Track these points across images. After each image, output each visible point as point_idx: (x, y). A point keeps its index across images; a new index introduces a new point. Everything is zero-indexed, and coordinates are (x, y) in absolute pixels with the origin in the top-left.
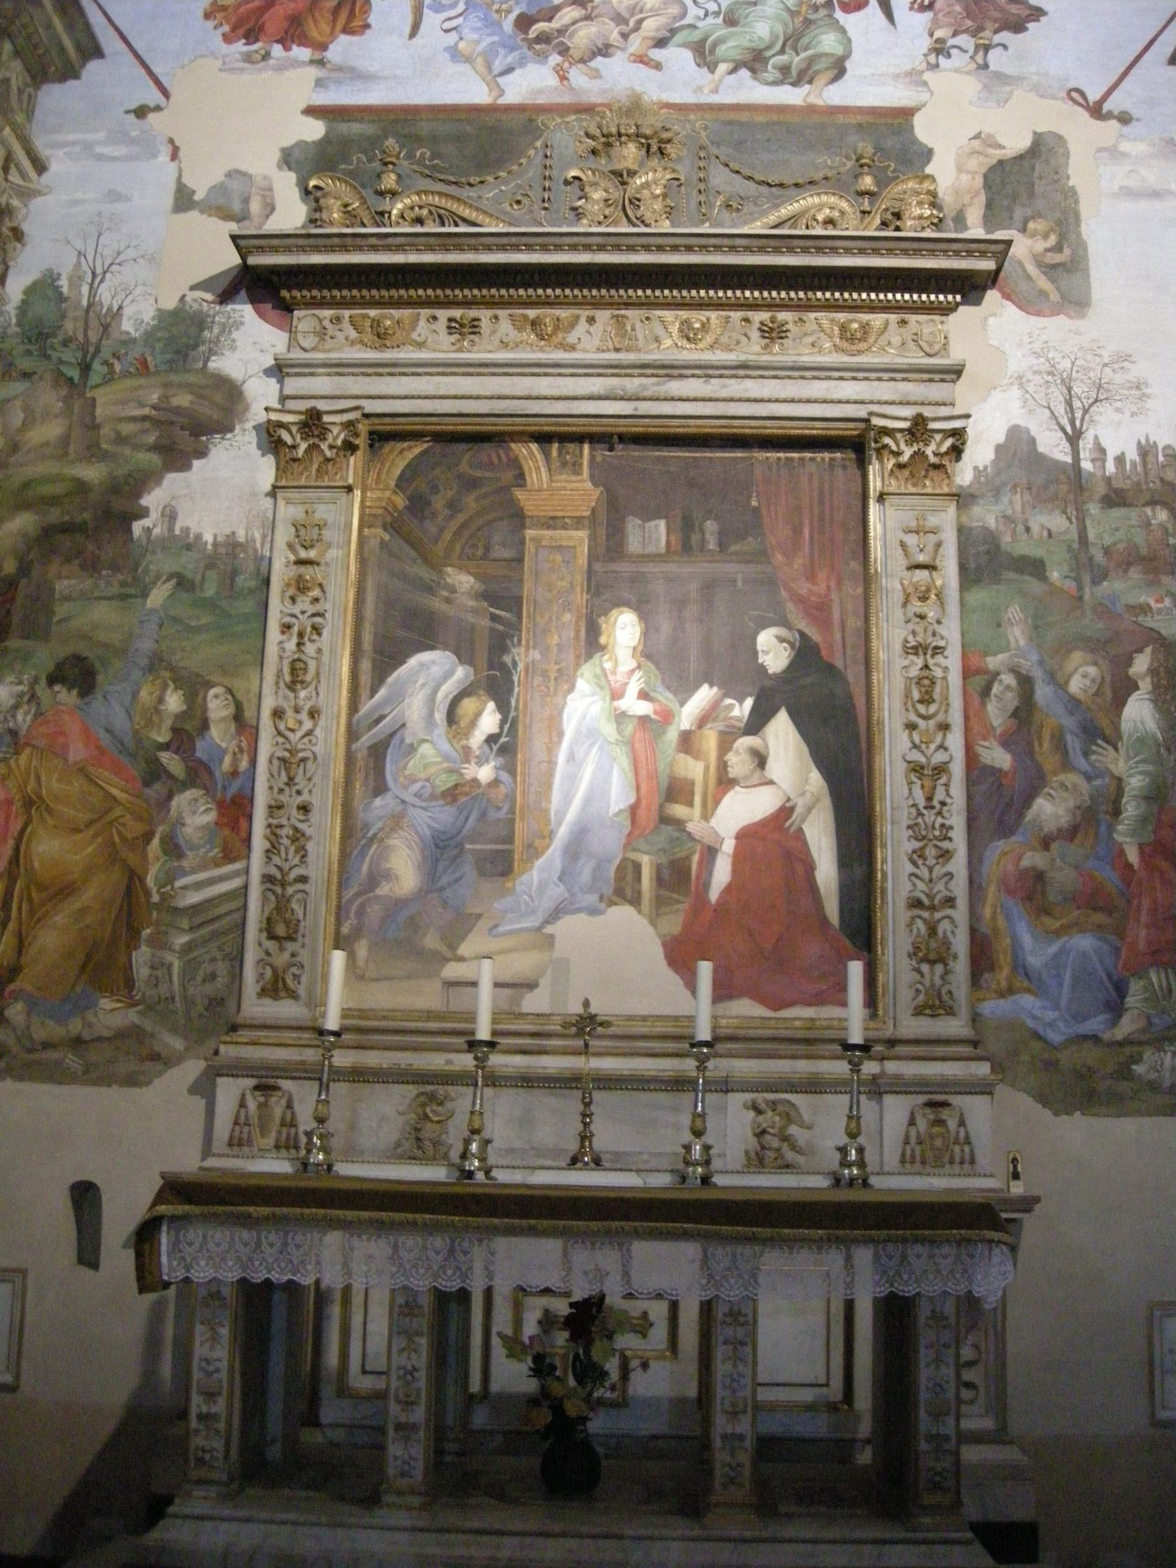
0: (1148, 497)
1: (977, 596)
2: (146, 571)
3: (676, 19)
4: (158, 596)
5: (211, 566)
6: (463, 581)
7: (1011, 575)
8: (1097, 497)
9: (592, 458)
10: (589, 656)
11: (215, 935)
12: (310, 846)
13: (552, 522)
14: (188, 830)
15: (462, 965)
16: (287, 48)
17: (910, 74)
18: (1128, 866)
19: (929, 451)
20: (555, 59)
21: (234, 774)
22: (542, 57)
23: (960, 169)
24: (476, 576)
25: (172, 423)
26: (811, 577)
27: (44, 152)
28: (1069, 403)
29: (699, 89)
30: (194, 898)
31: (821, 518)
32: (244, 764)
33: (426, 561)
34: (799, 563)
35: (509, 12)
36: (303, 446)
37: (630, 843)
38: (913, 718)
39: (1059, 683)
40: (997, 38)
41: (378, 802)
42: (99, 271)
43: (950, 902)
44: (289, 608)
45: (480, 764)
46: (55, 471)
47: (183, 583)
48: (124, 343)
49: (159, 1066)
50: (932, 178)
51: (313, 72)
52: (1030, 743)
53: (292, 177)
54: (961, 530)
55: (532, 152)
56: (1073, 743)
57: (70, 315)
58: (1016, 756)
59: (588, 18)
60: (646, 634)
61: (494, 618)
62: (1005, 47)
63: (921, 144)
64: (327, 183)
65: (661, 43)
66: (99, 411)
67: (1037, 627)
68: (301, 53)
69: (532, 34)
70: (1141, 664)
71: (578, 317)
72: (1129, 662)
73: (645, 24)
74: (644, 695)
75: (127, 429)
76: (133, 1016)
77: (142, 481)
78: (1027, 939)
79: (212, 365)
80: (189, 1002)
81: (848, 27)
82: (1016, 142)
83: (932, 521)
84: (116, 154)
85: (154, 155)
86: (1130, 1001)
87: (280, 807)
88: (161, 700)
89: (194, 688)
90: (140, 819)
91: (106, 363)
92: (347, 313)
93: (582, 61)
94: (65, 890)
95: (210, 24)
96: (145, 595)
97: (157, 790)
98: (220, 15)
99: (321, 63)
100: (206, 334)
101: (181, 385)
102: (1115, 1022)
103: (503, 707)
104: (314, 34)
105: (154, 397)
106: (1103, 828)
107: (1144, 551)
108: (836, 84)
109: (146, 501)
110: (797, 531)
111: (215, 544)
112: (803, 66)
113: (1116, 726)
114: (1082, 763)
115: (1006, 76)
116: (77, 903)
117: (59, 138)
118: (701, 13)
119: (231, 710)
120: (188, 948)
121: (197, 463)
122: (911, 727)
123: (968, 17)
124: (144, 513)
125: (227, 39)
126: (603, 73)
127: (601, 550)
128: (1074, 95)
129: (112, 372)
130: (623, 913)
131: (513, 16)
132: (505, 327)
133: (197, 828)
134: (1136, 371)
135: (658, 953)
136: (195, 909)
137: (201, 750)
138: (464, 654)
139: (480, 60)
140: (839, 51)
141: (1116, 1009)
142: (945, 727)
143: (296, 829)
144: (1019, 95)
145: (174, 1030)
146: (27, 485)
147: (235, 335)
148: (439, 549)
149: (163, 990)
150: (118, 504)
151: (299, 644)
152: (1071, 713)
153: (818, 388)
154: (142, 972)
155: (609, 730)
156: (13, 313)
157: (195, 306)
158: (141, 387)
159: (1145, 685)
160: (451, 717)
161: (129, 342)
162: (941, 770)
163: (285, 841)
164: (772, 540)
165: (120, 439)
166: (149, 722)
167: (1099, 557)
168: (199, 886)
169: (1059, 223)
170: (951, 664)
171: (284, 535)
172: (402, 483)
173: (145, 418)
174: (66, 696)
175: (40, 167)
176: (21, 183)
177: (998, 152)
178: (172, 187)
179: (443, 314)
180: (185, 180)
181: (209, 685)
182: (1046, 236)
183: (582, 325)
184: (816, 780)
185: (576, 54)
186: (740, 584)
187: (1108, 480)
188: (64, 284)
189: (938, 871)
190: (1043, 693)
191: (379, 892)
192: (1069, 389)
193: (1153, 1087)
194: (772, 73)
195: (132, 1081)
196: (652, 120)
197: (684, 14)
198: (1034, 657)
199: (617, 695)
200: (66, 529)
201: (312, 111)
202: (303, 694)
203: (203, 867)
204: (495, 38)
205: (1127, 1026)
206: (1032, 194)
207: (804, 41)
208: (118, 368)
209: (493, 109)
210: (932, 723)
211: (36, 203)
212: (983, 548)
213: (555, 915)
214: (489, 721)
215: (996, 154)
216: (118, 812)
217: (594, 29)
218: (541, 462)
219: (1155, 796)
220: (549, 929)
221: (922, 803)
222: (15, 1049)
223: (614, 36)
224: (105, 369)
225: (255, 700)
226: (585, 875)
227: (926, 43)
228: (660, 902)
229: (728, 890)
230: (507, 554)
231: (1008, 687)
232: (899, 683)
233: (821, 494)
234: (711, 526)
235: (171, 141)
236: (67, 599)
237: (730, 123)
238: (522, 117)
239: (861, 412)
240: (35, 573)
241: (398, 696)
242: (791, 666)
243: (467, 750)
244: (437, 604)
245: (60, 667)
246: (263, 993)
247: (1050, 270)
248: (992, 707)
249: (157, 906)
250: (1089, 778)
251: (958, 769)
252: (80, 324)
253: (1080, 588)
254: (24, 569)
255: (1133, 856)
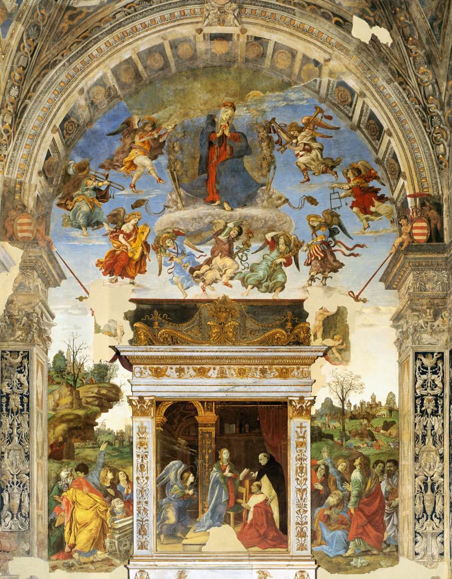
0: (361, 416)
1: (314, 445)
2: (99, 441)
3: (236, 270)
4: (103, 447)
5: (116, 439)
6: (183, 441)
7: (325, 439)
8: (348, 417)
9: (216, 407)
10: (216, 462)
11: (125, 535)
12: (148, 512)
13: (205, 425)
14: (117, 509)
15: (187, 540)
16: (123, 278)
17: (303, 288)
18: (351, 514)
19: (304, 406)
20: (201, 284)
21: (128, 494)
22: (197, 283)
23: (316, 319)
24: (186, 440)
25: (102, 398)
26: (273, 439)
27: (53, 311)
28: (343, 391)
29: (242, 295)
30: (120, 526)
31: (276, 423)
32: (130, 492)
33: (173, 436)
34: (270, 435)
35: (187, 267)
36: (139, 406)
37: (228, 510)
38: (298, 477)
39: (335, 467)
40: (330, 275)
41: (164, 500)
42: (75, 351)
43: (306, 523)
44: (138, 450)
45: (189, 490)
46: (70, 412)
47: (109, 444)
48: (85, 374)
49: (114, 567)
50: (309, 323)
51: (132, 287)
52: (327, 483)
53: (128, 322)
54: (312, 427)
55: (195, 316)
56: (338, 483)
57: (68, 365)
58: (324, 486)
59: (210, 269)
60: (230, 455)
61: (191, 451)
62: (331, 278)
63: (306, 312)
64: (137, 325)
65: (232, 278)
66: (81, 395)
67: (330, 453)
68: (127, 280)
69: (194, 275)
70: (357, 462)
71: (210, 368)
72: (354, 461)
73: (227, 271)
74: (230, 471)
75: (89, 400)
76: (106, 556)
77: (96, 415)
78: (325, 532)
79: (111, 381)
80: (120, 551)
81: (286, 272)
82: (333, 310)
83: (303, 425)
84: (75, 313)
85: (87, 314)
86: (350, 547)
87: (140, 502)
88: (107, 475)
89: (115, 471)
90: (104, 506)
91: (81, 380)
92: (148, 366)
93: (209, 284)
94: (86, 525)
95: (98, 268)
96: (99, 447)
97: (107, 499)
98: (101, 265)
99: (133, 283)
100: (108, 372)
101: (103, 387)
102: (346, 552)
103: (195, 475)
104: (130, 273)
105: (96, 390)
106: (345, 504)
107: (360, 432)
108: (283, 291)
109: (97, 421)
110: (269, 427)
111: (117, 433)
112: (273, 286)
113: (350, 479)
114: (341, 488)
115: (331, 288)
116: (89, 528)
117: (57, 307)
118: (243, 267)
119: (126, 477)
120: (119, 538)
121: (109, 410)
122: (297, 479)
123: (321, 267)
124: (97, 424)
125: (105, 274)
126: (215, 288)
127: (219, 433)
128: (351, 293)
129: (83, 383)
130: (226, 527)
131: (189, 268)
132: (192, 372)
133: (119, 508)
134: (361, 381)
135: (235, 536)
136: (120, 529)
137: (118, 488)
138: (184, 461)
139: (179, 284)
140: (283, 280)
141: (347, 549)
142: (306, 479)
143: (145, 508)
144: (336, 294)
145: (117, 558)
146: (63, 416)
147: (117, 372)
148: (176, 433)
149: (114, 549)
150: (90, 422)
151: (142, 460)
152: (338, 475)
153: (275, 388)
154: (108, 545)
155: (222, 481)
156: (51, 364)
157: (105, 363)
158: (92, 387)
159: (358, 467)
160: (182, 478)
161: (87, 374)
162: (305, 489)
163: (142, 511)
164: (263, 430)
165: (88, 403)
166: (104, 481)
167: (348, 433)
168: (121, 523)
169: (343, 336)
170: (308, 463)
171: (135, 430)
172: (165, 414)
173: (94, 397)
174: (81, 475)
175: (53, 317)
176: (46, 321)
177: (328, 313)
178: (93, 325)
179: (174, 367)
180: (99, 323)
181: (119, 471)
182: (339, 340)
183: (212, 371)
184: (274, 492)
185: (207, 282)
186: (254, 442)
187: (351, 412)
188: (65, 354)
189: (303, 516)
190: (331, 470)
191: (165, 522)
192: (342, 387)
193: (355, 567)
194: (263, 289)
195: (107, 571)
196: (230, 305)
197: (238, 268)
198: (329, 461)
199: (224, 471)
200: (76, 428)
201: (132, 300)
202: (144, 473)
203: (122, 518)
204: (184, 276)
205: (350, 552)
206: (336, 327)
207: (273, 277)
208: (84, 381)
209: (184, 301)
210: (303, 478)
211: (53, 328)
212: (317, 432)
213: (209, 527)
214: (191, 479)
215: (327, 314)
216: (98, 504)
217: (212, 273)
218: (202, 407)
219: (359, 496)
220: (208, 531)
221: (300, 499)
222: (76, 564)
223: (218, 276)
224: (81, 382)
225: (131, 475)
226: (217, 518)
227: (308, 277)
228: (236, 524)
229: (252, 520)
230: (194, 434)
231: (322, 469)
232: (295, 468)
233: (276, 416)
234: (247, 426)
235: (91, 309)
236: (78, 448)
237: (252, 306)
238: (194, 303)
239: (287, 394)
240: (68, 441)
241: (167, 472)
242: (267, 464)
243: (186, 488)
244: (176, 448)
245: (78, 467)
246: (139, 548)
247: (340, 351)
248: (318, 474)
249: (110, 528)
250: (342, 491)
251: (309, 490)
252: (72, 368)
253: (342, 442)
254: (65, 440)
255: (352, 511)
